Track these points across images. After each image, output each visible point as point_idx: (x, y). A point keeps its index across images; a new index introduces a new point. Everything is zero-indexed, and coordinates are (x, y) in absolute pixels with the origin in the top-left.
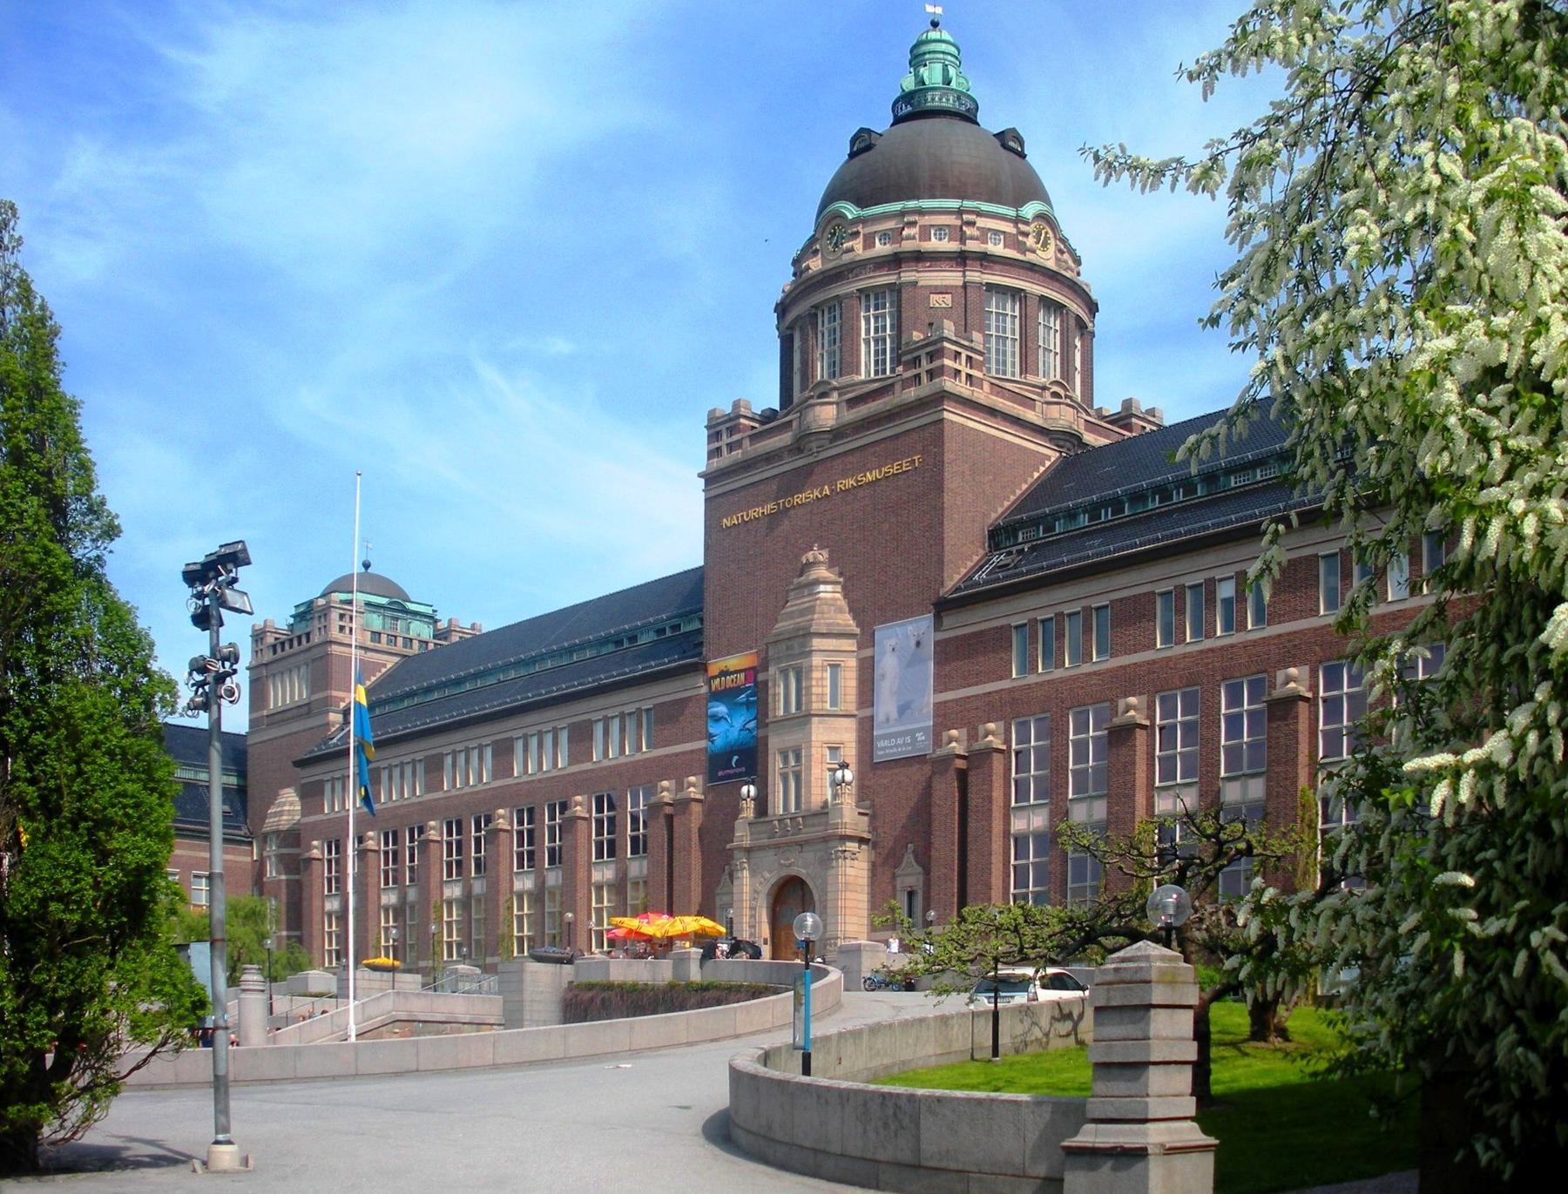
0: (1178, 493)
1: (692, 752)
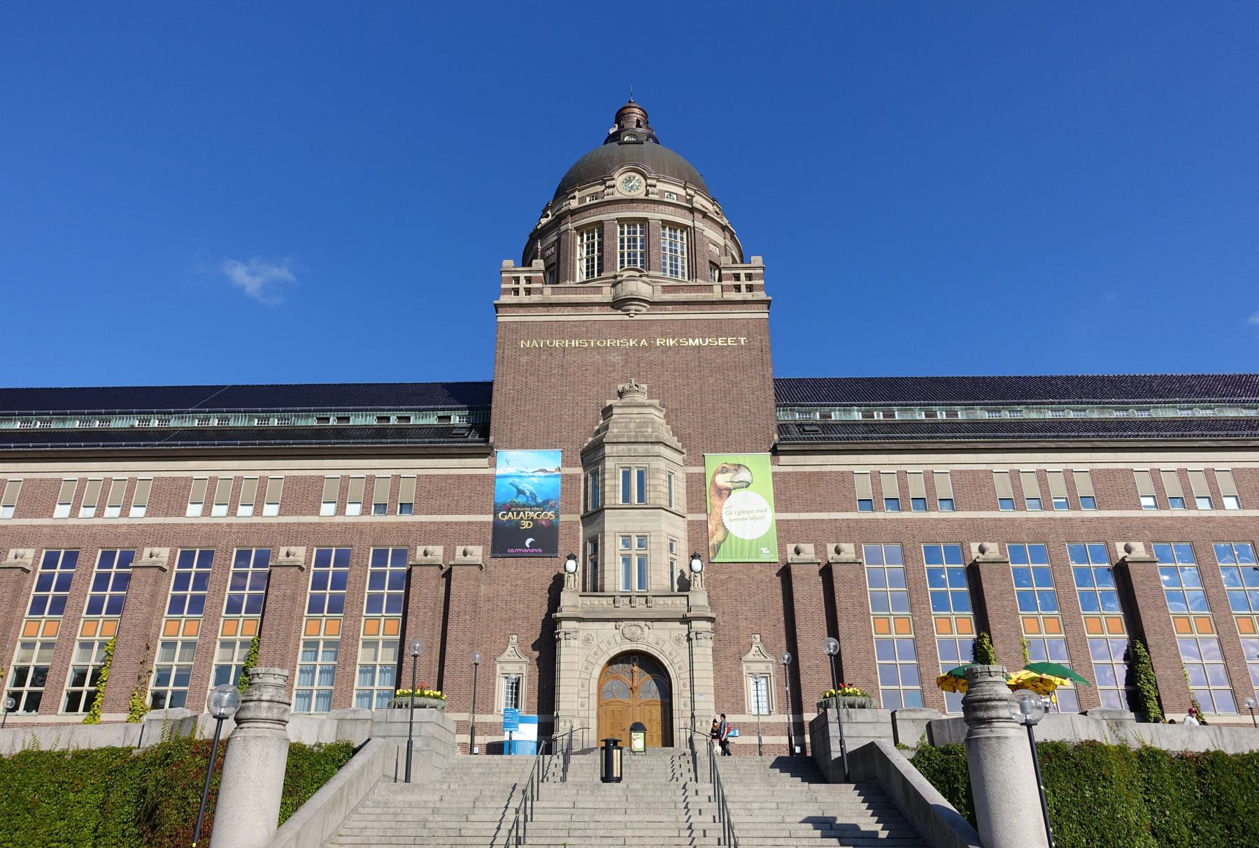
0: (941, 414)
1: (469, 523)
